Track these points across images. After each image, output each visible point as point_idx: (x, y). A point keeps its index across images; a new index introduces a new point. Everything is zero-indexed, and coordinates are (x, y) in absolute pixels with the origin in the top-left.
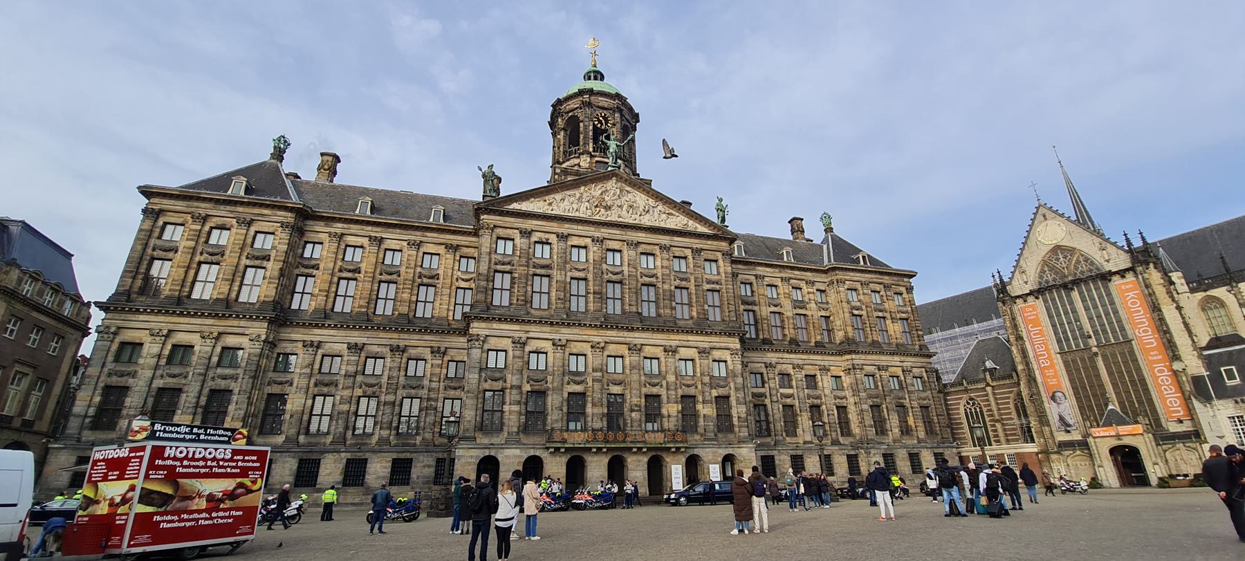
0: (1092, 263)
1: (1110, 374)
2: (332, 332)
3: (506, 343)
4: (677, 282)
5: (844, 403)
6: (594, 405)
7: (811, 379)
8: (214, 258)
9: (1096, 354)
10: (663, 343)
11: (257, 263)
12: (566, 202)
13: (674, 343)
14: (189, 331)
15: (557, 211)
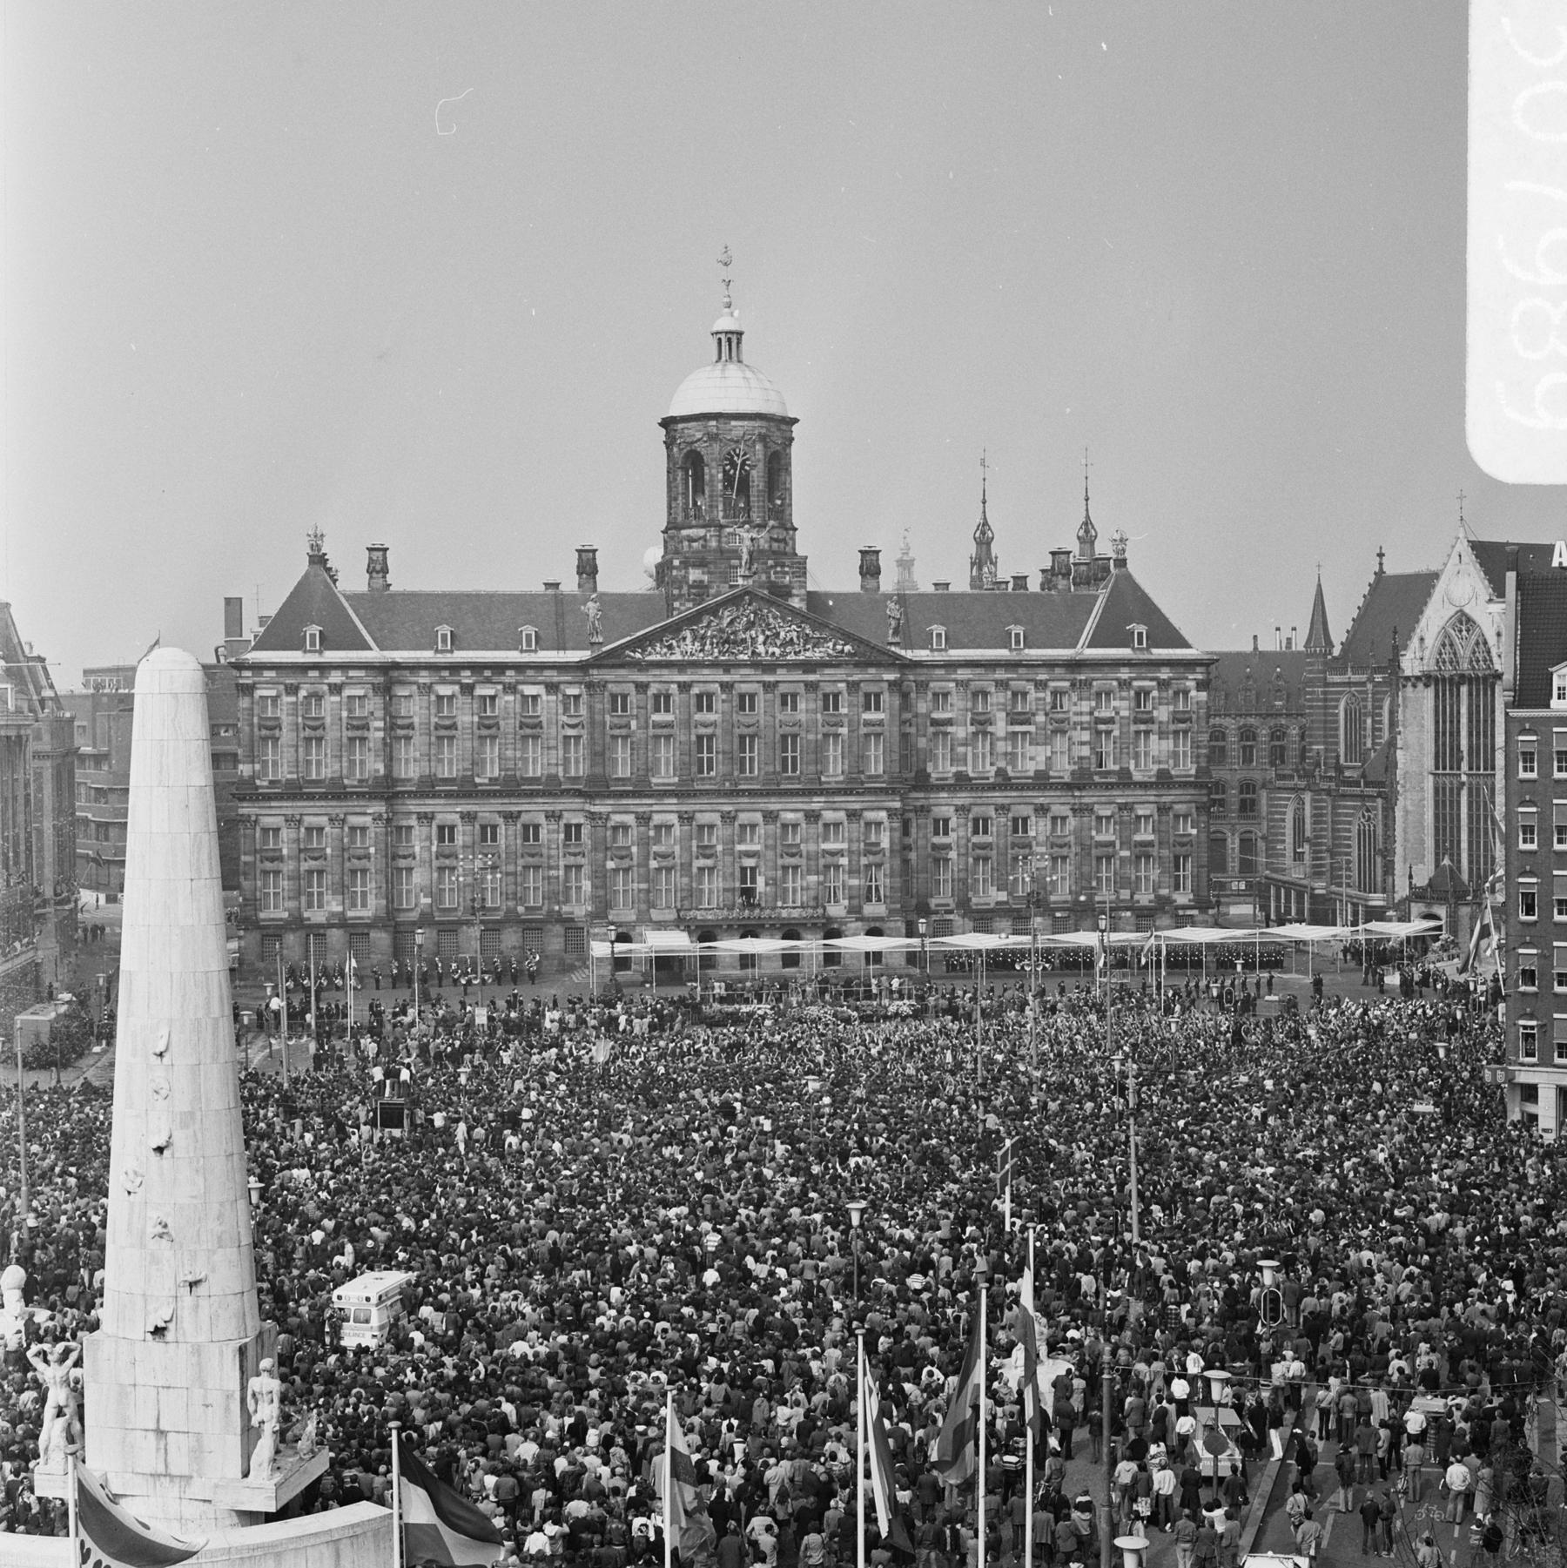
0: (1489, 652)
1: (1470, 817)
2: (442, 801)
3: (630, 819)
4: (827, 729)
5: (1065, 851)
6: (724, 879)
7: (1020, 824)
8: (319, 733)
9: (1463, 784)
10: (805, 807)
11: (358, 733)
12: (688, 641)
13: (815, 806)
14: (316, 814)
15: (677, 657)
